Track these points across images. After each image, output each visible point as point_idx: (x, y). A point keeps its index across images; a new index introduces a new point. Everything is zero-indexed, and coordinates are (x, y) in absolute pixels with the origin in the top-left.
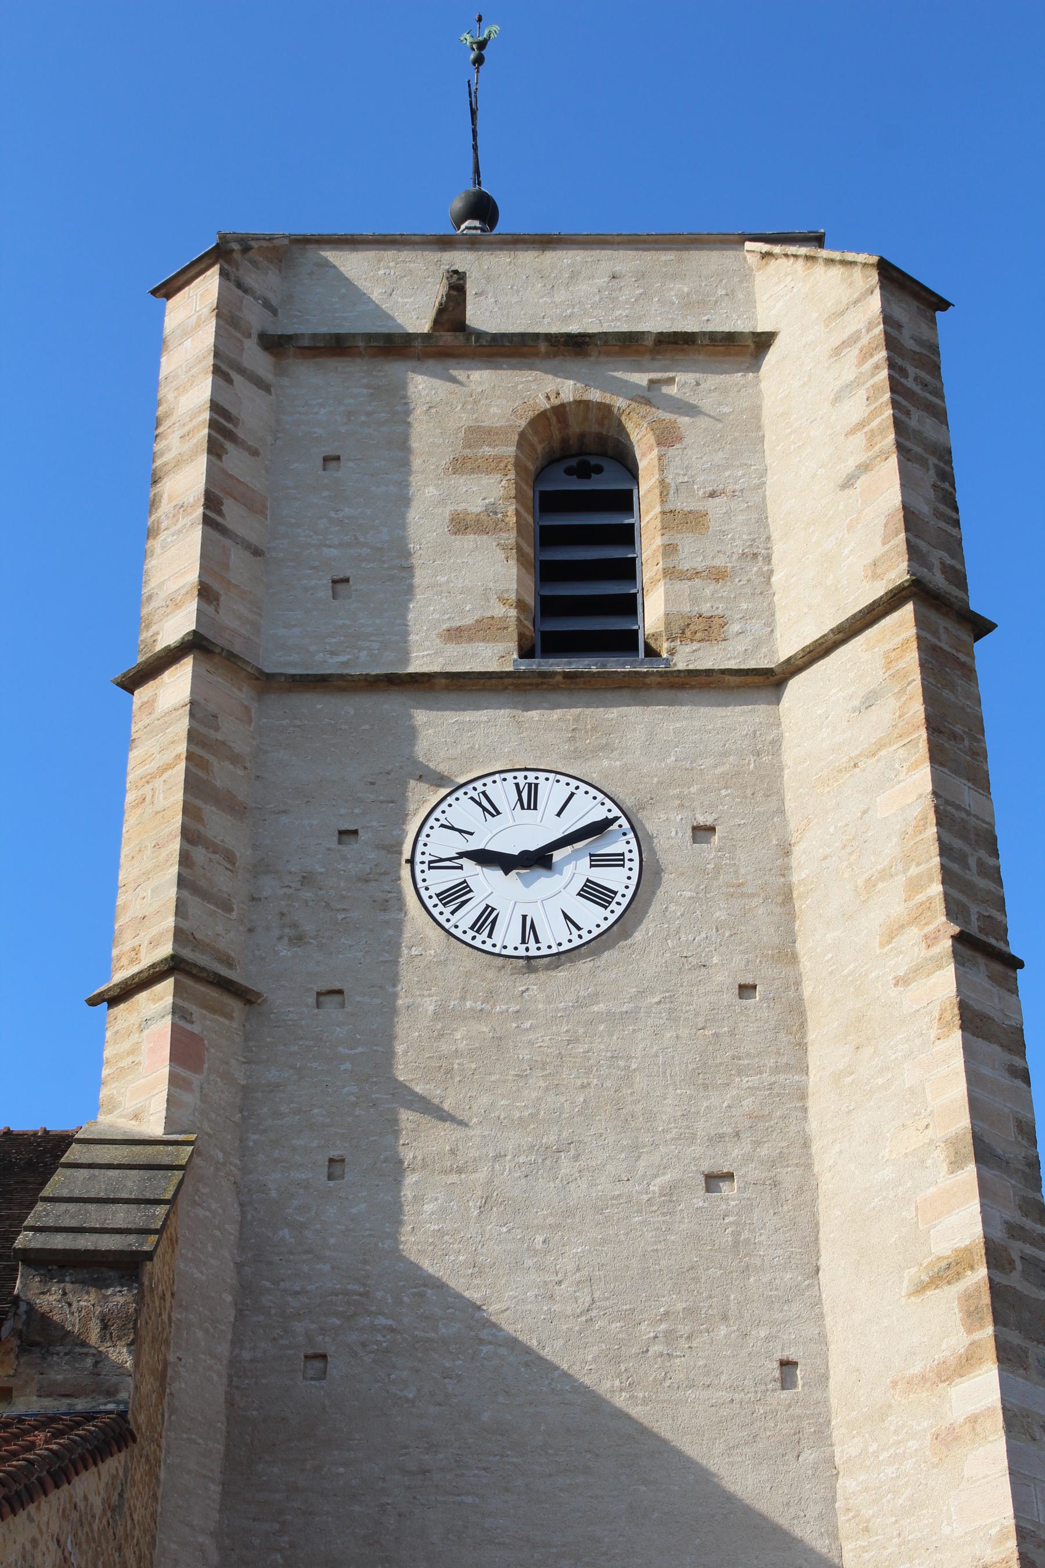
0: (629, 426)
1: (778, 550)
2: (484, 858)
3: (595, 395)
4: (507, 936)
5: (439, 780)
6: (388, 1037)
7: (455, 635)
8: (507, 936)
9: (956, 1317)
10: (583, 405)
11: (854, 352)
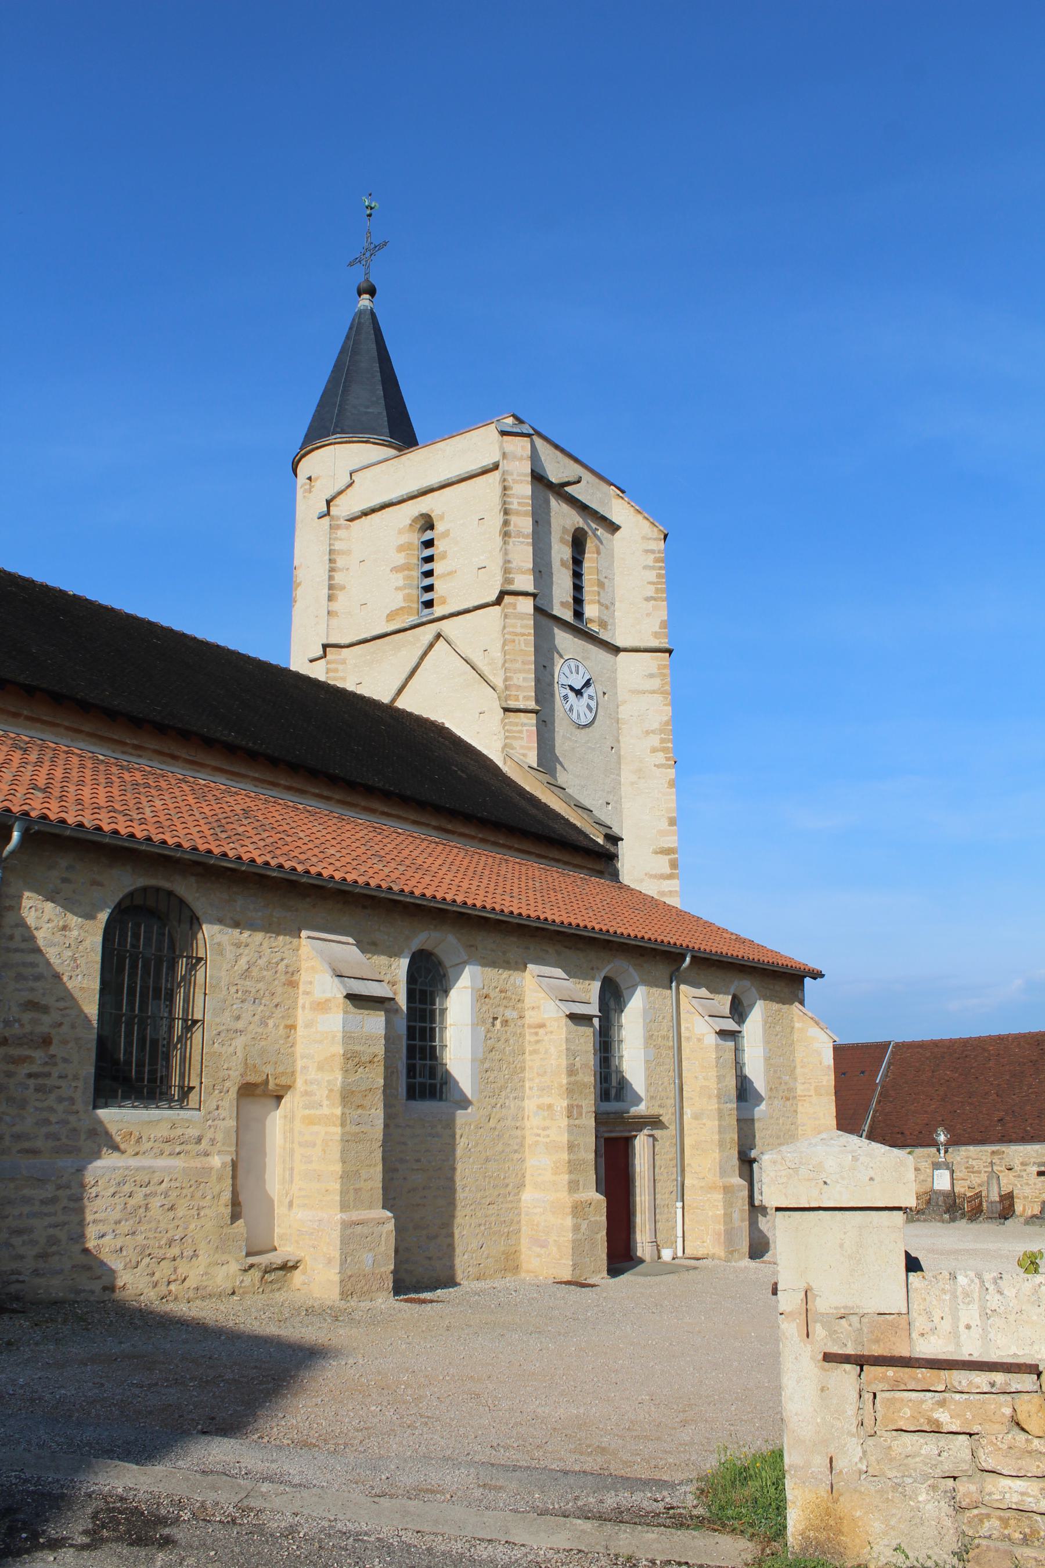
0: (588, 541)
1: (617, 604)
2: (572, 688)
3: (586, 528)
4: (574, 716)
5: (561, 656)
6: (554, 739)
7: (563, 604)
8: (574, 716)
9: (667, 864)
10: (583, 529)
11: (652, 556)
